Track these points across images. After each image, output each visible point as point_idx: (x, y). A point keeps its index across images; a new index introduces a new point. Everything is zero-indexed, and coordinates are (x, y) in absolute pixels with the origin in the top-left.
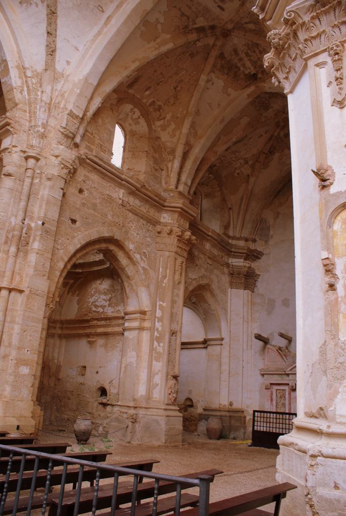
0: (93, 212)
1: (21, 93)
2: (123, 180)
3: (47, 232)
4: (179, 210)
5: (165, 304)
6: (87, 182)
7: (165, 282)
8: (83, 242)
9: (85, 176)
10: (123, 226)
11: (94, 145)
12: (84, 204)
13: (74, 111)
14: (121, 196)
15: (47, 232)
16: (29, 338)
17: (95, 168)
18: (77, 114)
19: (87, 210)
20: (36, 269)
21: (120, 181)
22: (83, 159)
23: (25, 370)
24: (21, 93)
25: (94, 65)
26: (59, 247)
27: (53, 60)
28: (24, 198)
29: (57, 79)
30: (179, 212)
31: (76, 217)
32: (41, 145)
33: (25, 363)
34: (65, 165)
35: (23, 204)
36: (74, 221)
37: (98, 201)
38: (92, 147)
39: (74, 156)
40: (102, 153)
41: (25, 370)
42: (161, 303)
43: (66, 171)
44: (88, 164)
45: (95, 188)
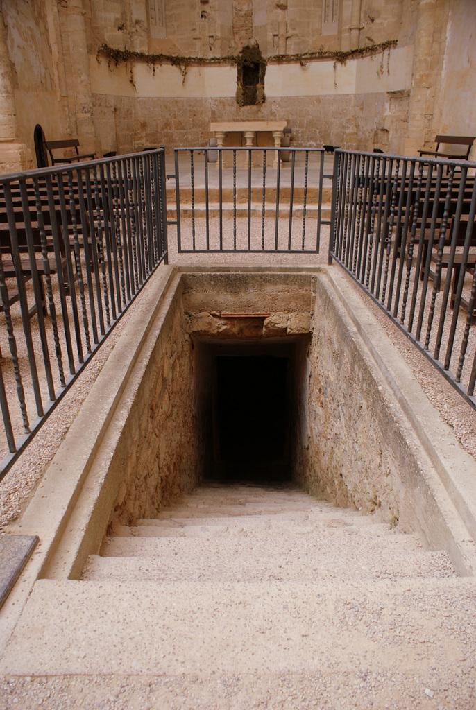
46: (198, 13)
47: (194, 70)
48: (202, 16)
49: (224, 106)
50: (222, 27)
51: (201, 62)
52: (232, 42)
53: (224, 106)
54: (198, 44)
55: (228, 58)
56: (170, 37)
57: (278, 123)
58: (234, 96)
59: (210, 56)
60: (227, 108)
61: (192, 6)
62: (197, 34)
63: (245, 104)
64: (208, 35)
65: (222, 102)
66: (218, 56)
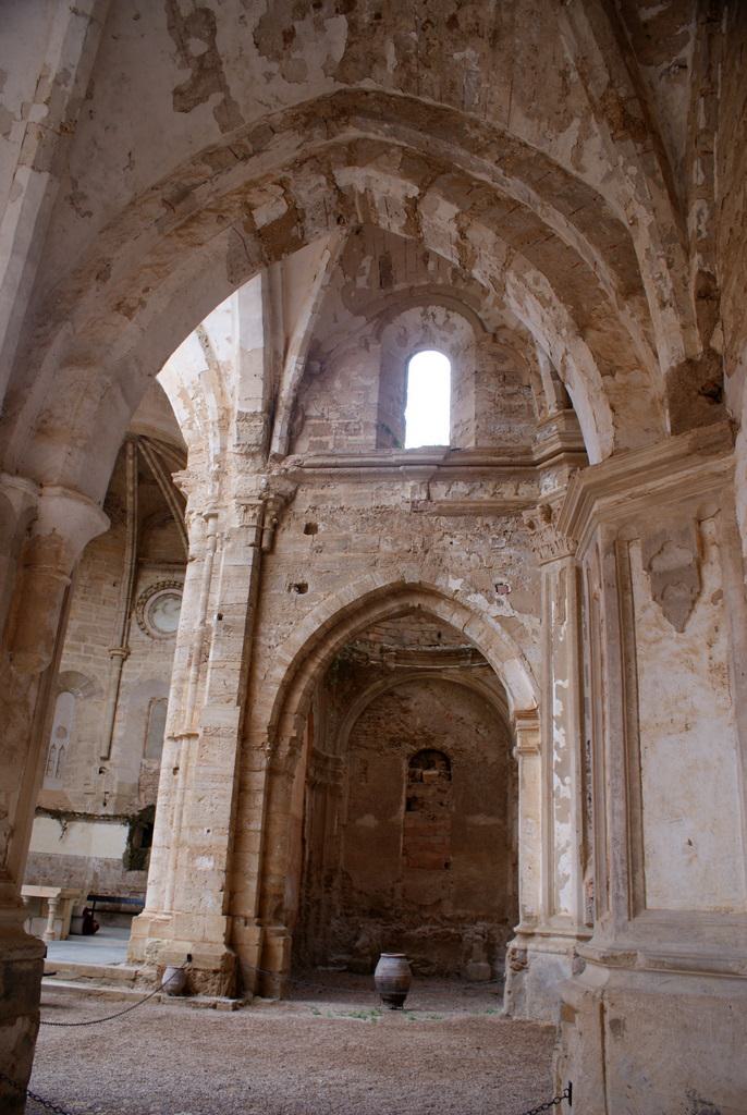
0: (342, 554)
1: (190, 428)
2: (399, 466)
3: (227, 628)
4: (562, 455)
5: (567, 681)
6: (321, 506)
7: (562, 632)
8: (324, 618)
9: (316, 497)
10: (426, 552)
11: (331, 433)
12: (320, 547)
13: (245, 410)
14: (408, 496)
15: (227, 628)
16: (209, 810)
17: (331, 475)
18: (252, 410)
19: (327, 555)
20: (212, 694)
21: (392, 469)
22: (294, 473)
23: (206, 863)
24: (190, 428)
25: (241, 320)
26: (273, 643)
27: (211, 352)
28: (203, 586)
29: (226, 374)
30: (568, 460)
31: (306, 577)
32: (216, 492)
33: (206, 851)
34: (247, 506)
35: (202, 594)
36: (302, 588)
37: (352, 529)
38: (324, 439)
39: (264, 481)
40: (350, 438)
41: (206, 863)
42: (560, 682)
43: (251, 513)
44: (313, 475)
45: (342, 508)
46: (95, 769)
47: (78, 828)
48: (100, 772)
49: (108, 868)
50: (121, 784)
51: (89, 817)
52: (136, 799)
53: (108, 868)
54: (90, 799)
55: (119, 816)
56: (65, 789)
57: (52, 889)
58: (121, 857)
59: (103, 812)
60: (113, 871)
61: (89, 762)
62: (90, 789)
63: (131, 868)
64: (103, 791)
65: (107, 864)
66: (111, 813)
